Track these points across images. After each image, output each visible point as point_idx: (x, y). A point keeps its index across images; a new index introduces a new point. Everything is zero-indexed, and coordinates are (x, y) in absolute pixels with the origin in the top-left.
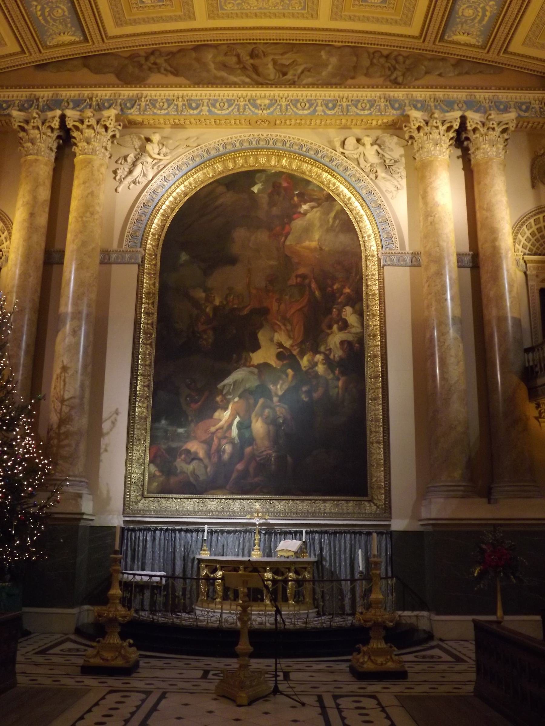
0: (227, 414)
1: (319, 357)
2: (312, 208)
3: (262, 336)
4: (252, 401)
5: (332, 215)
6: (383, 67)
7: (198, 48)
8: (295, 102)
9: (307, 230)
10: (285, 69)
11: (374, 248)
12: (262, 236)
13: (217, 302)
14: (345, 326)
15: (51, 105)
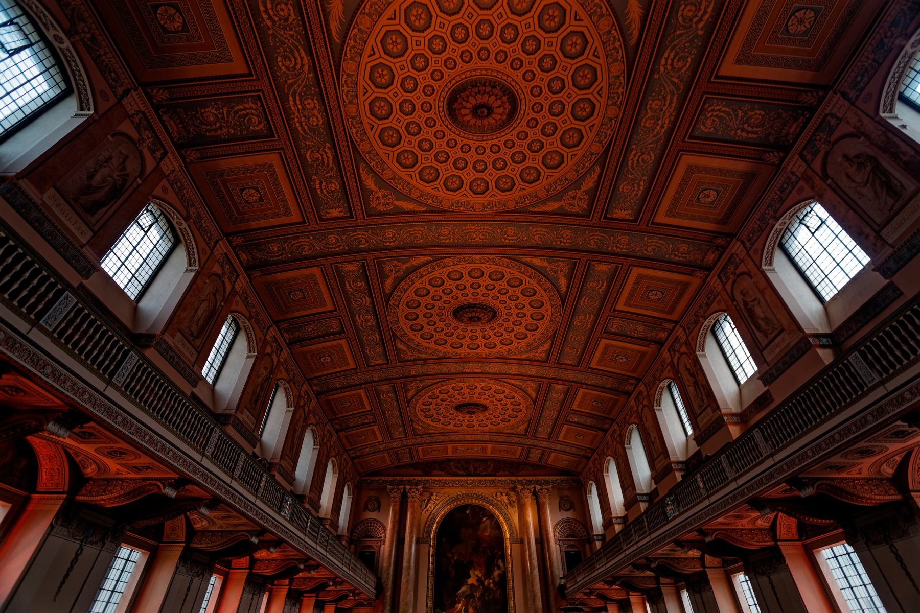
0: (460, 605)
1: (491, 581)
3: (471, 573)
7: (449, 460)
9: (485, 529)
14: (499, 568)
15: (401, 483)
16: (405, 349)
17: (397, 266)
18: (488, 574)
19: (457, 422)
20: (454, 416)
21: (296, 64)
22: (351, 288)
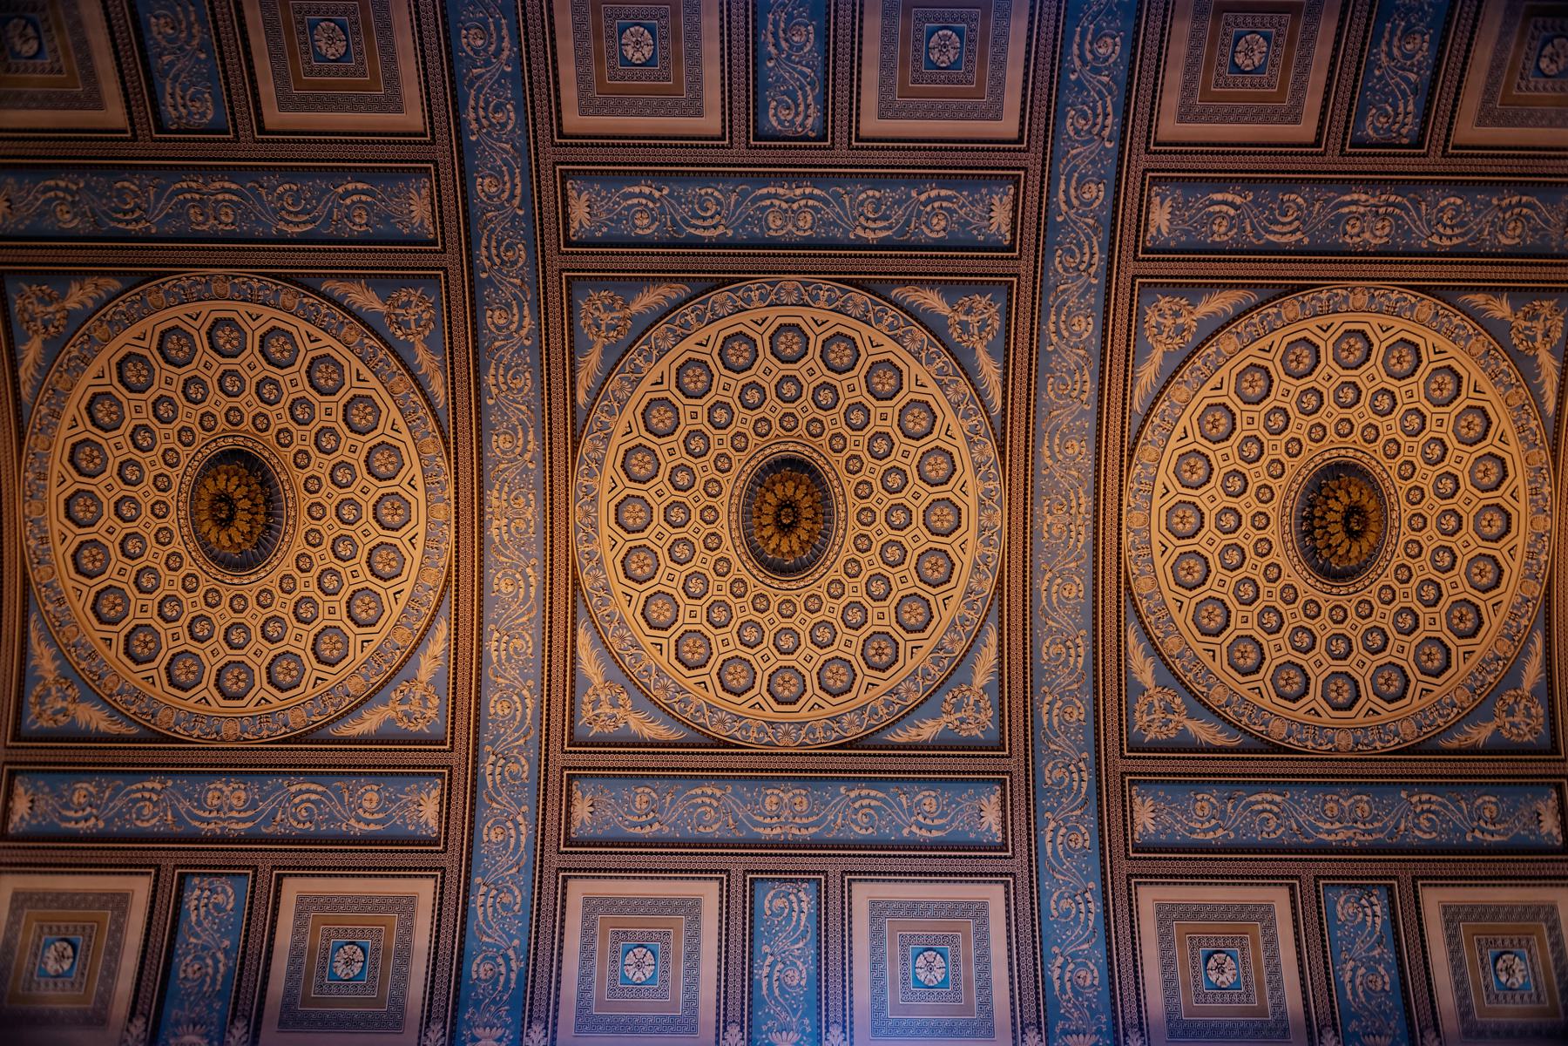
16: (1491, 727)
17: (1151, 705)
21: (710, 805)
22: (1214, 829)
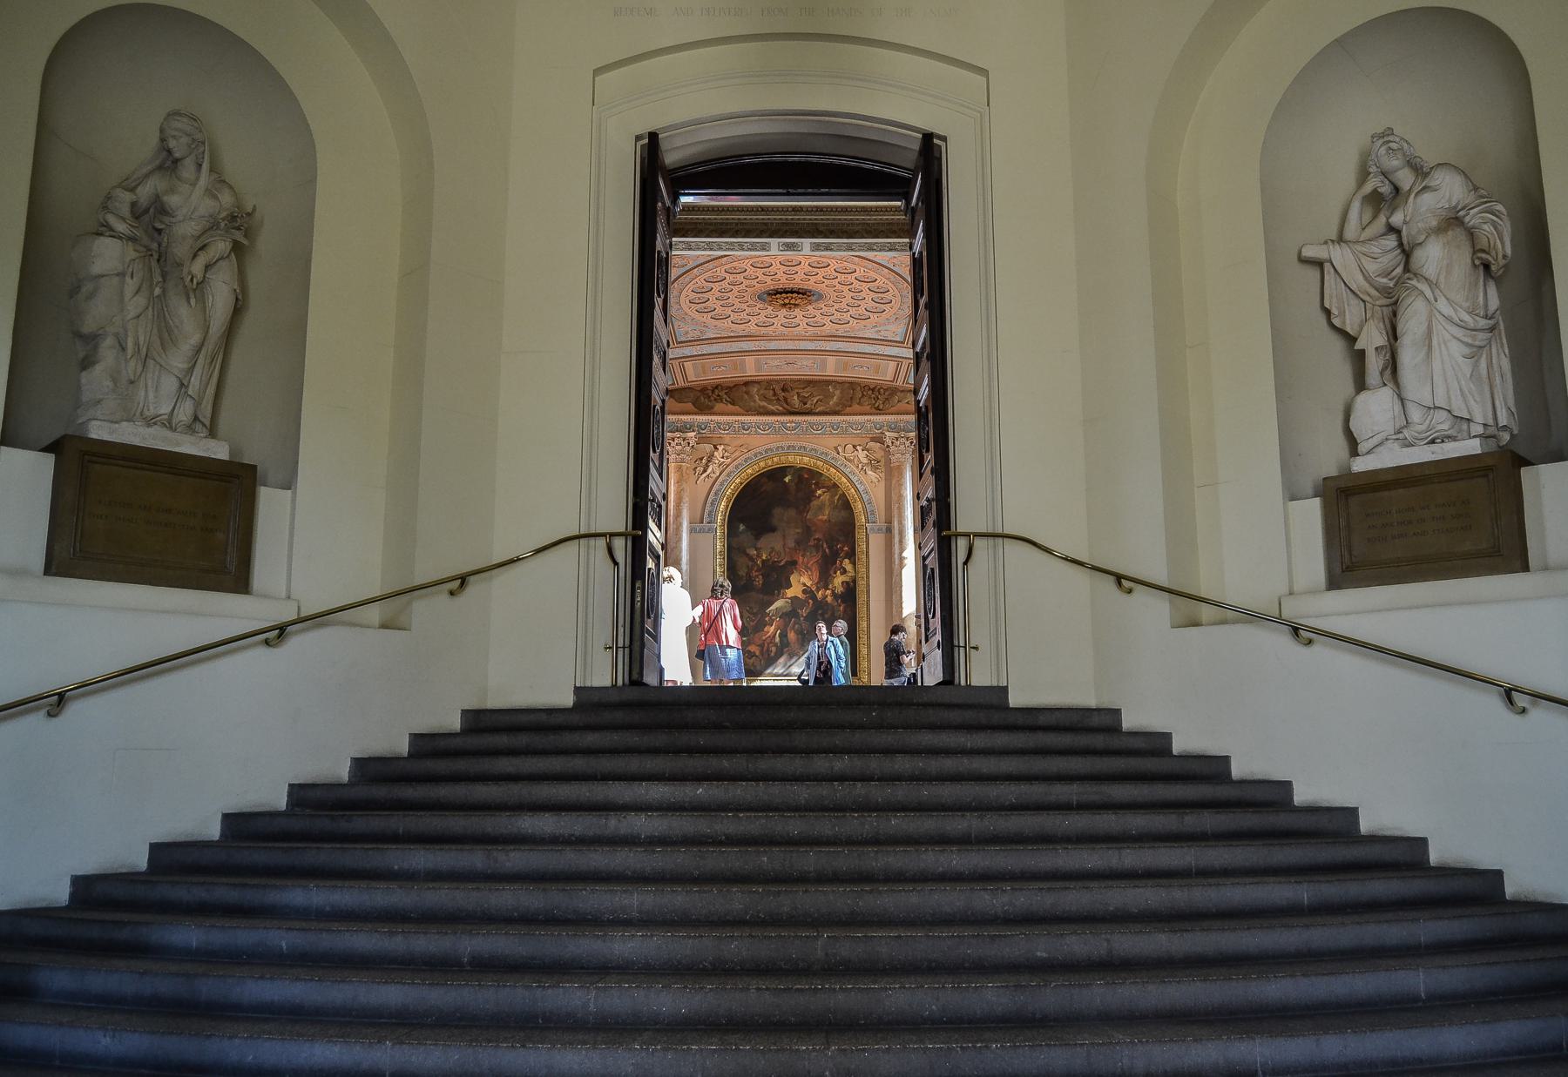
1: (828, 592)
2: (824, 493)
4: (787, 620)
5: (837, 497)
6: (870, 398)
7: (746, 384)
8: (811, 425)
9: (821, 508)
10: (806, 400)
11: (863, 520)
12: (792, 512)
13: (764, 558)
14: (844, 572)
18: (825, 579)
19: (762, 318)
20: (756, 310)
